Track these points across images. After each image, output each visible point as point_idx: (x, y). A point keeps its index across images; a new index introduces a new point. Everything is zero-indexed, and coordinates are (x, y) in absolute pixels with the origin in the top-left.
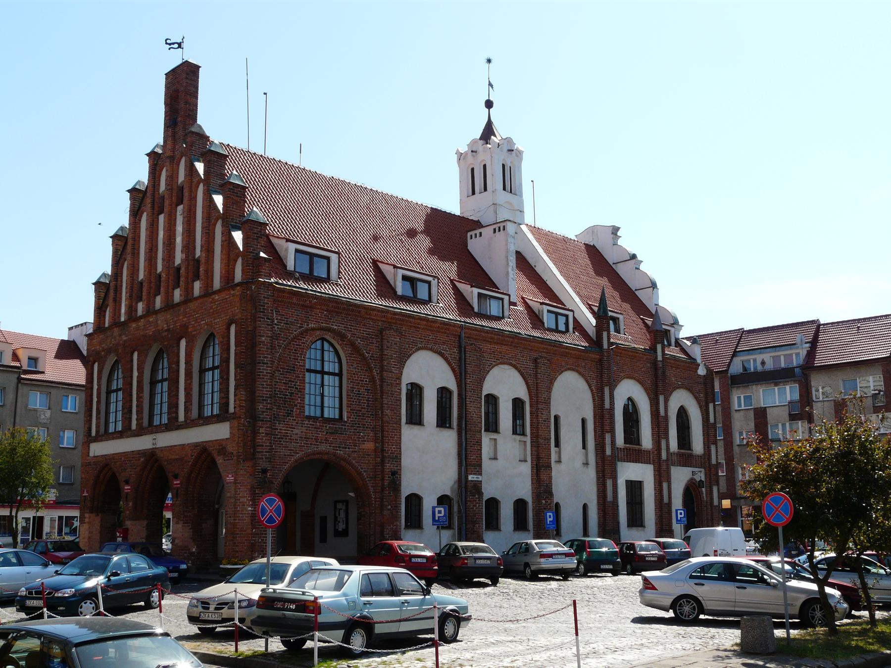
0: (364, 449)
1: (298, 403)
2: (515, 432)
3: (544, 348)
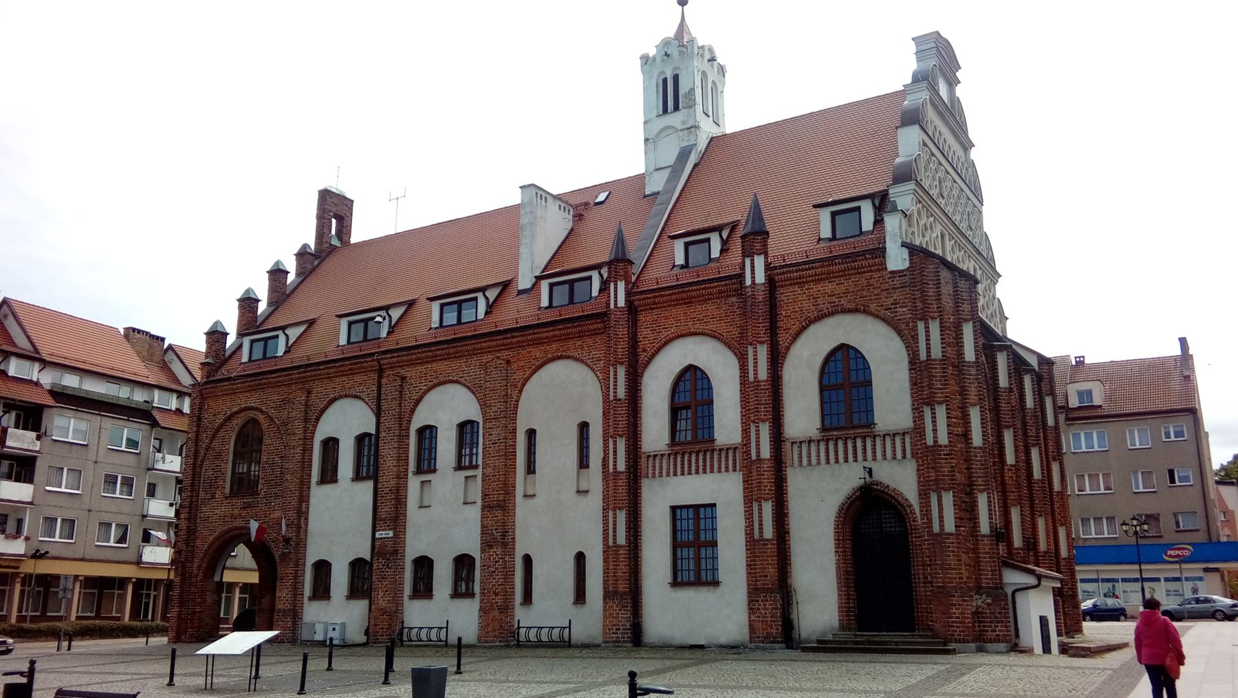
0: (274, 518)
1: (221, 485)
2: (459, 467)
3: (499, 346)
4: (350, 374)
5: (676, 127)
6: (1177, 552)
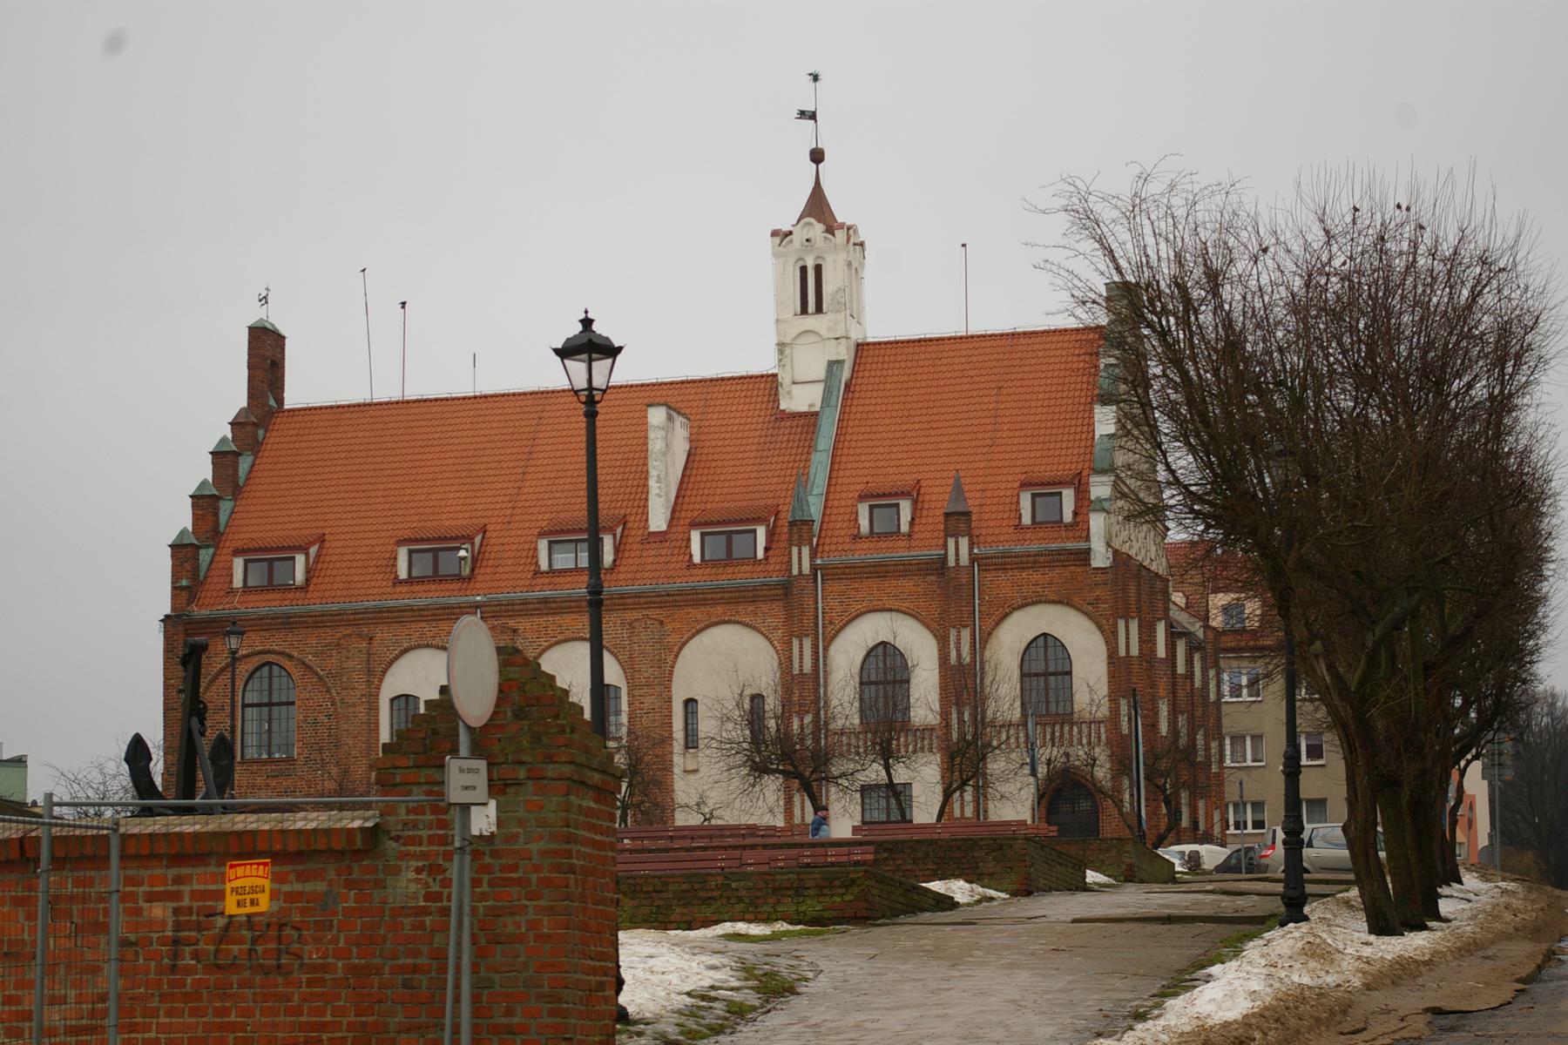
4: (434, 620)
5: (821, 333)
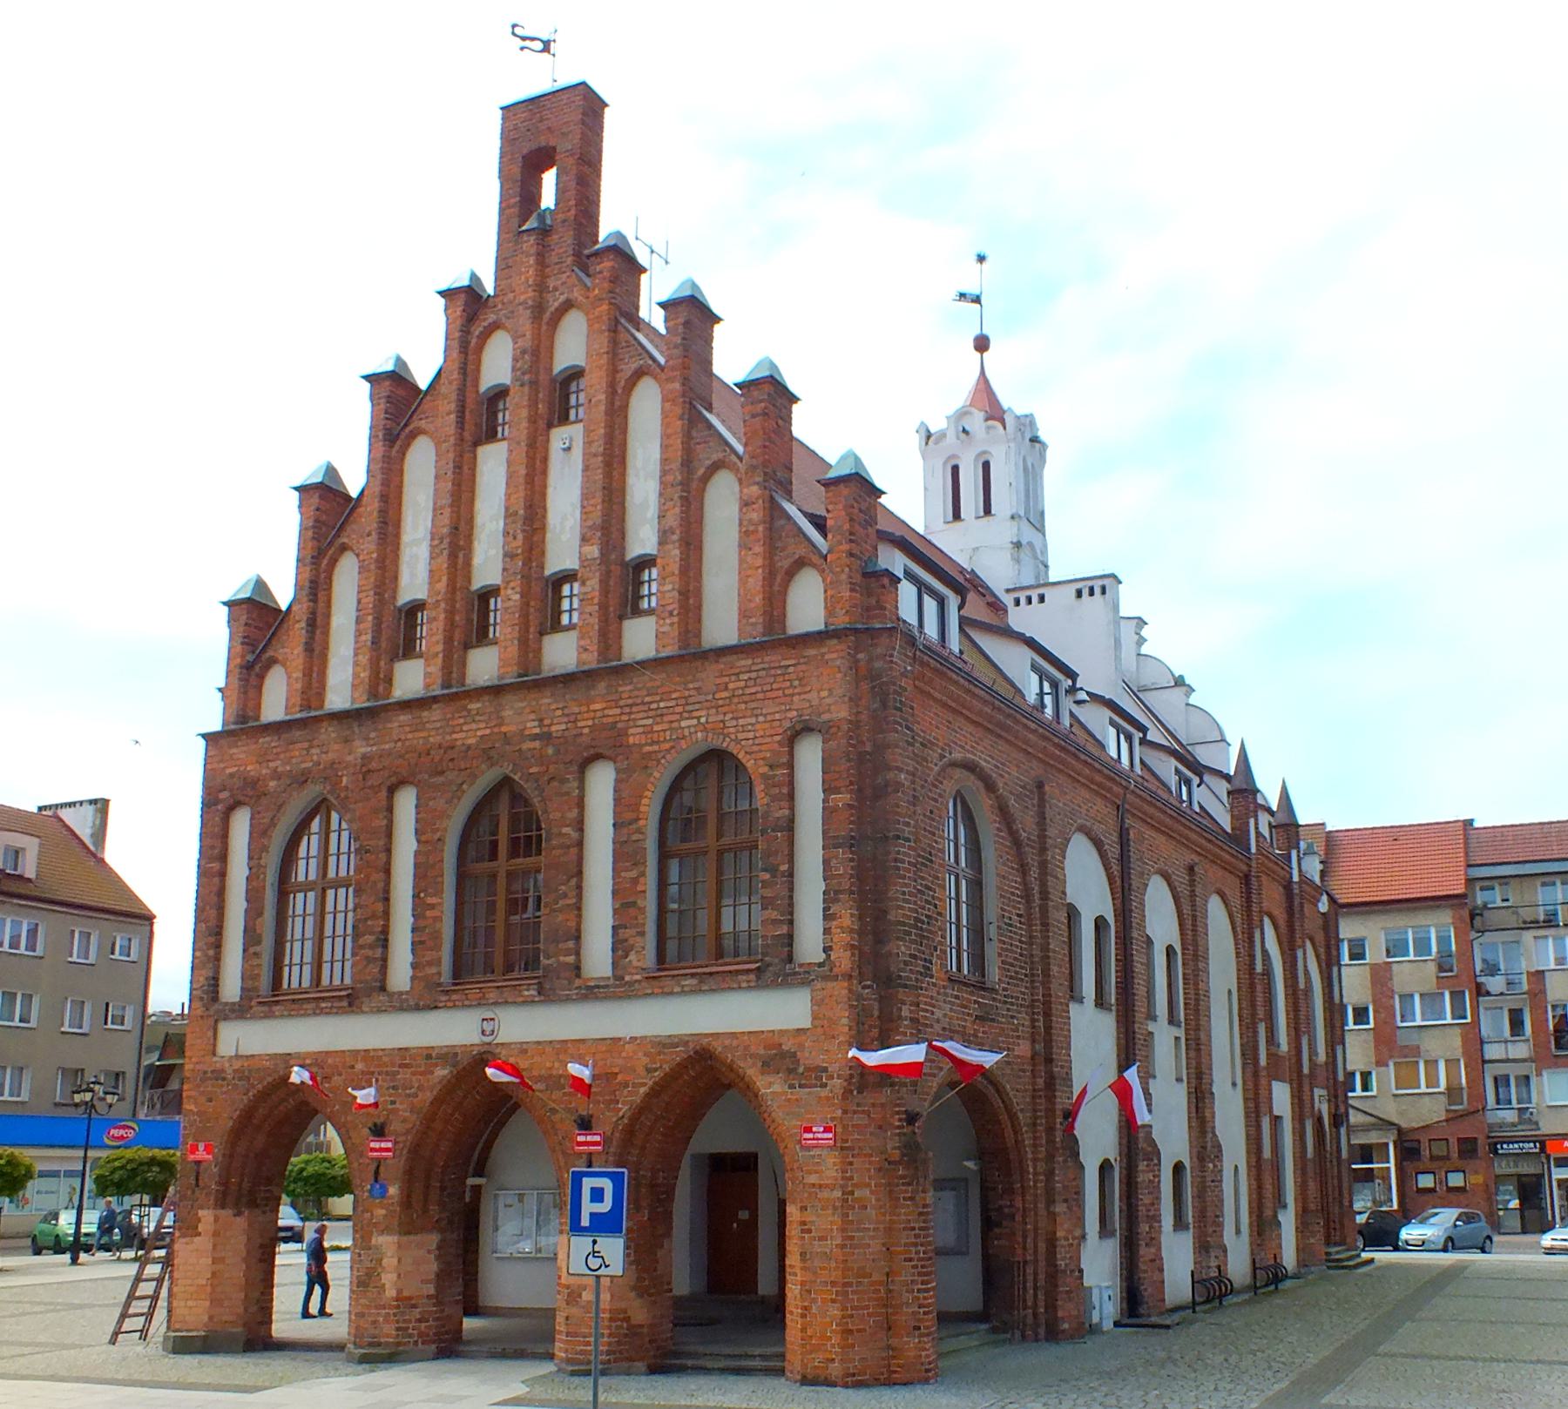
6: (122, 1132)
